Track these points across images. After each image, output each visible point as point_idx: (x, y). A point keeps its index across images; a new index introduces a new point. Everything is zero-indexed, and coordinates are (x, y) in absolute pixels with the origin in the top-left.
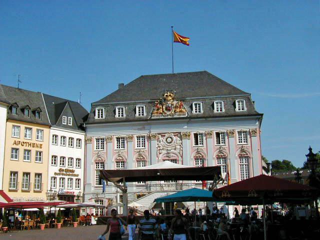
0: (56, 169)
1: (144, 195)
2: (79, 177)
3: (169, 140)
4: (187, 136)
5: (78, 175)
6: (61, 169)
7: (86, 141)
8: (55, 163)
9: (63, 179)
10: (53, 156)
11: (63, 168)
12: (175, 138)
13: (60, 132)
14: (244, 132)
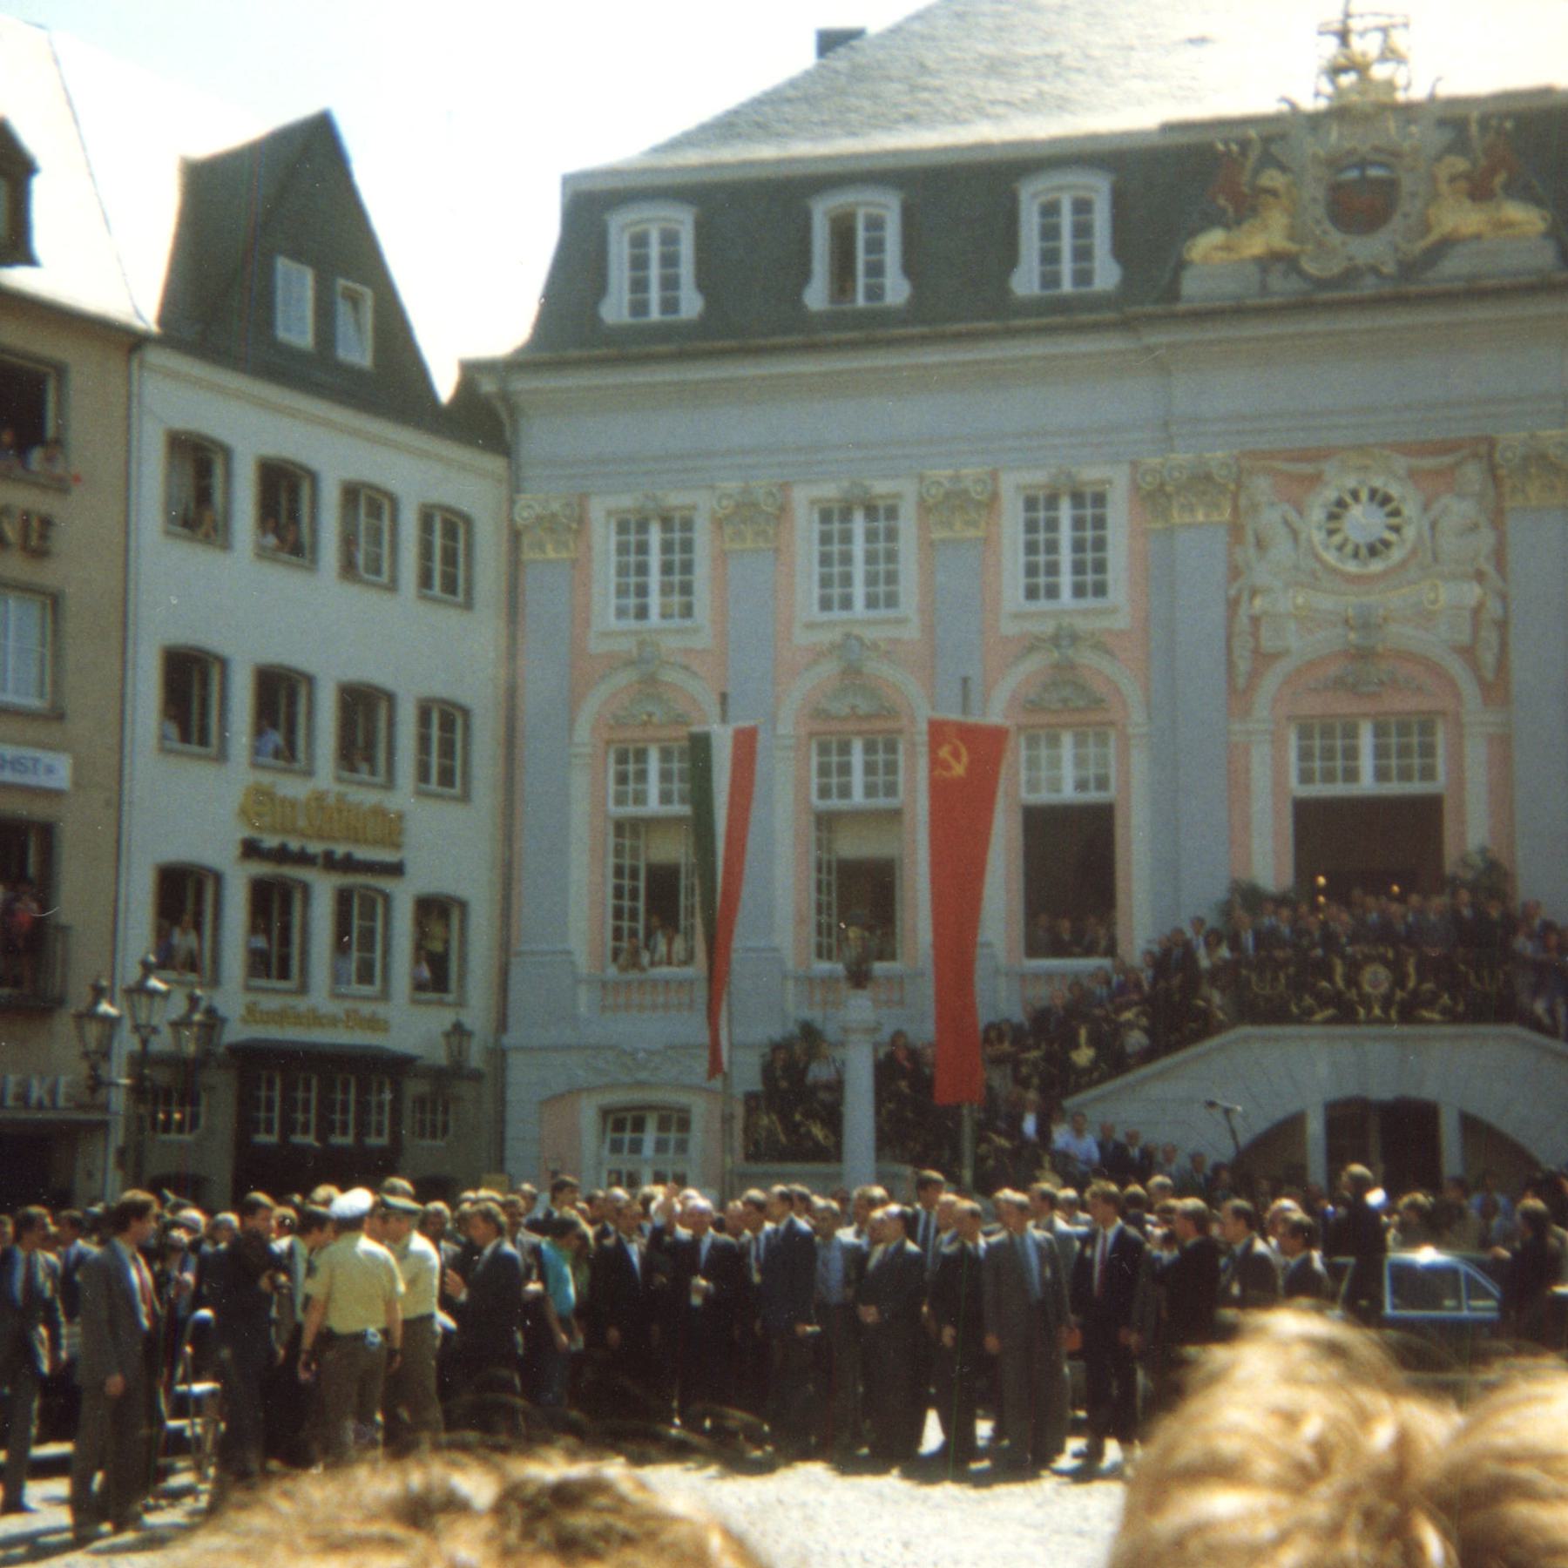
3: (1363, 521)
7: (516, 536)
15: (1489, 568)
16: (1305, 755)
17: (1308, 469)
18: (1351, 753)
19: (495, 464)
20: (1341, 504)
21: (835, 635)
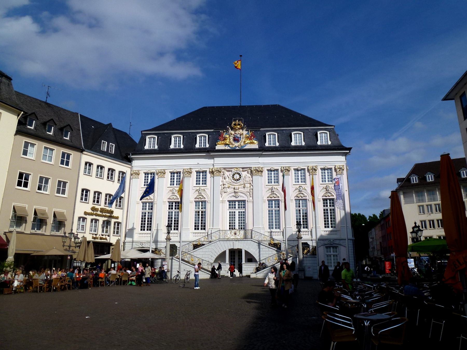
0: (88, 207)
1: (204, 245)
2: (119, 220)
3: (237, 177)
4: (259, 171)
5: (117, 218)
6: (93, 207)
8: (86, 200)
9: (96, 221)
10: (83, 190)
11: (97, 207)
12: (244, 174)
13: (96, 160)
14: (328, 169)
15: (251, 182)
16: (230, 205)
17: (231, 170)
18: (235, 205)
19: (130, 166)
20: (234, 174)
21: (171, 189)
